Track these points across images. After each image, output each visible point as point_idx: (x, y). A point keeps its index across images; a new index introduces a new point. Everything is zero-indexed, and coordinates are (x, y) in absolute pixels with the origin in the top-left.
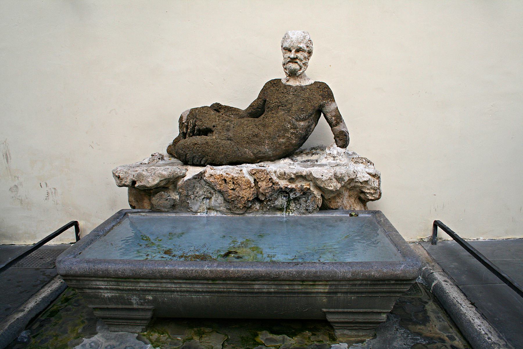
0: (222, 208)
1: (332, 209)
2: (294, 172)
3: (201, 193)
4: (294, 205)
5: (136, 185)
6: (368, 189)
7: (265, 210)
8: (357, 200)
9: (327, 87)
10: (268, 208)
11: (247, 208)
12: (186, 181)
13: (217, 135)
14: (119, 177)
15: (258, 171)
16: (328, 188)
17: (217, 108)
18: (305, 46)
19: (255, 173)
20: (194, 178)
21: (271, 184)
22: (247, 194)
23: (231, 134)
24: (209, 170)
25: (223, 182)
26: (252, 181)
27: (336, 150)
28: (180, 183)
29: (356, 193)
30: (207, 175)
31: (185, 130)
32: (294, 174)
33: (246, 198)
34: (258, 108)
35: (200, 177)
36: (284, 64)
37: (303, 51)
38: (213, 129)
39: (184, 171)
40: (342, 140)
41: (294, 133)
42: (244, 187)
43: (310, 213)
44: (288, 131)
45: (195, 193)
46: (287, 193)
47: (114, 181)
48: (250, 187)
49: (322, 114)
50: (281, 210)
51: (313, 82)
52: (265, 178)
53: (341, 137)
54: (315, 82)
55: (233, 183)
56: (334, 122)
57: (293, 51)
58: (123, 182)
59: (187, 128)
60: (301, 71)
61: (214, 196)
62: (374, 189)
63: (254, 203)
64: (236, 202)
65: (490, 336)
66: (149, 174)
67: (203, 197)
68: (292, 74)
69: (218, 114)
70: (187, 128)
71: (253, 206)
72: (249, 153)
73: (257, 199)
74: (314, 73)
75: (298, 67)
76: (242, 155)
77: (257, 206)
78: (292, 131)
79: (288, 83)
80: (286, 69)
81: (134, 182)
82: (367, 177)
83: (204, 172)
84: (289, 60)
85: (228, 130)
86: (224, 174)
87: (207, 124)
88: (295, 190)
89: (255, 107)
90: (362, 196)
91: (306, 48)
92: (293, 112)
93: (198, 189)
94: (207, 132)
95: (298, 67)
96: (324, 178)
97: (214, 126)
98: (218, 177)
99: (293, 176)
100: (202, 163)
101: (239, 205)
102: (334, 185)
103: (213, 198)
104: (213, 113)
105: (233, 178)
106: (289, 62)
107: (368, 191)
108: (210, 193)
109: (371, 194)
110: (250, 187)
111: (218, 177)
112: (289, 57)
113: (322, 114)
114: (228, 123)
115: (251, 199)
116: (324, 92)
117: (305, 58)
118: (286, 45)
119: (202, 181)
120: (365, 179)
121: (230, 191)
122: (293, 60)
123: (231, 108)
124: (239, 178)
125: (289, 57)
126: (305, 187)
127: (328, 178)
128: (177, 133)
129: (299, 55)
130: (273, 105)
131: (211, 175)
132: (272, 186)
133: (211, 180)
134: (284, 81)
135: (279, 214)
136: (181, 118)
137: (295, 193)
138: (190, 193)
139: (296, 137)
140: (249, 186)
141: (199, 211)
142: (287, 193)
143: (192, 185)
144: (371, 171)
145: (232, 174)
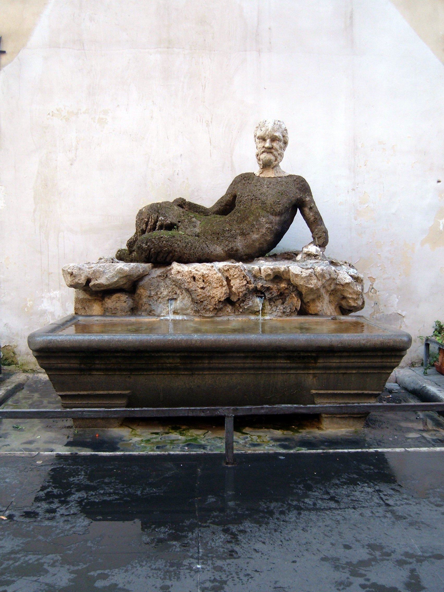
0: (189, 311)
1: (312, 314)
2: (272, 267)
3: (165, 293)
4: (269, 307)
5: (91, 284)
6: (350, 294)
7: (236, 313)
8: (338, 309)
9: (303, 180)
10: (241, 310)
11: (218, 310)
14: (72, 274)
16: (308, 285)
18: (281, 136)
19: (228, 270)
22: (219, 293)
24: (176, 266)
25: (192, 279)
29: (337, 298)
30: (173, 271)
31: (144, 226)
32: (272, 270)
34: (226, 205)
35: (165, 276)
36: (258, 155)
37: (279, 140)
40: (321, 238)
42: (215, 285)
43: (287, 316)
44: (263, 226)
45: (159, 293)
46: (262, 293)
48: (222, 286)
49: (298, 210)
50: (256, 313)
52: (239, 275)
55: (203, 281)
56: (312, 218)
57: (268, 141)
59: (147, 225)
60: (276, 163)
61: (181, 297)
62: (357, 294)
64: (205, 302)
67: (167, 299)
68: (266, 165)
70: (147, 225)
71: (224, 309)
72: (219, 250)
73: (228, 301)
74: (289, 165)
75: (273, 158)
76: (212, 252)
77: (229, 309)
79: (262, 176)
80: (259, 160)
81: (89, 281)
82: (348, 279)
83: (171, 269)
88: (272, 289)
89: (223, 204)
90: (344, 303)
91: (282, 138)
92: (266, 209)
93: (162, 289)
95: (273, 158)
98: (187, 273)
100: (168, 260)
101: (209, 307)
102: (314, 283)
103: (179, 299)
104: (176, 208)
105: (203, 276)
106: (263, 152)
107: (350, 296)
109: (355, 300)
110: (222, 286)
111: (187, 273)
113: (298, 210)
115: (222, 299)
117: (281, 147)
118: (259, 133)
119: (167, 279)
120: (347, 281)
121: (199, 290)
123: (195, 205)
124: (210, 275)
127: (308, 274)
128: (131, 232)
129: (275, 145)
131: (179, 272)
132: (245, 285)
133: (179, 277)
134: (257, 174)
135: (253, 317)
137: (271, 293)
138: (153, 293)
139: (271, 233)
140: (221, 284)
141: (162, 314)
142: (262, 293)
143: (156, 284)
145: (202, 271)
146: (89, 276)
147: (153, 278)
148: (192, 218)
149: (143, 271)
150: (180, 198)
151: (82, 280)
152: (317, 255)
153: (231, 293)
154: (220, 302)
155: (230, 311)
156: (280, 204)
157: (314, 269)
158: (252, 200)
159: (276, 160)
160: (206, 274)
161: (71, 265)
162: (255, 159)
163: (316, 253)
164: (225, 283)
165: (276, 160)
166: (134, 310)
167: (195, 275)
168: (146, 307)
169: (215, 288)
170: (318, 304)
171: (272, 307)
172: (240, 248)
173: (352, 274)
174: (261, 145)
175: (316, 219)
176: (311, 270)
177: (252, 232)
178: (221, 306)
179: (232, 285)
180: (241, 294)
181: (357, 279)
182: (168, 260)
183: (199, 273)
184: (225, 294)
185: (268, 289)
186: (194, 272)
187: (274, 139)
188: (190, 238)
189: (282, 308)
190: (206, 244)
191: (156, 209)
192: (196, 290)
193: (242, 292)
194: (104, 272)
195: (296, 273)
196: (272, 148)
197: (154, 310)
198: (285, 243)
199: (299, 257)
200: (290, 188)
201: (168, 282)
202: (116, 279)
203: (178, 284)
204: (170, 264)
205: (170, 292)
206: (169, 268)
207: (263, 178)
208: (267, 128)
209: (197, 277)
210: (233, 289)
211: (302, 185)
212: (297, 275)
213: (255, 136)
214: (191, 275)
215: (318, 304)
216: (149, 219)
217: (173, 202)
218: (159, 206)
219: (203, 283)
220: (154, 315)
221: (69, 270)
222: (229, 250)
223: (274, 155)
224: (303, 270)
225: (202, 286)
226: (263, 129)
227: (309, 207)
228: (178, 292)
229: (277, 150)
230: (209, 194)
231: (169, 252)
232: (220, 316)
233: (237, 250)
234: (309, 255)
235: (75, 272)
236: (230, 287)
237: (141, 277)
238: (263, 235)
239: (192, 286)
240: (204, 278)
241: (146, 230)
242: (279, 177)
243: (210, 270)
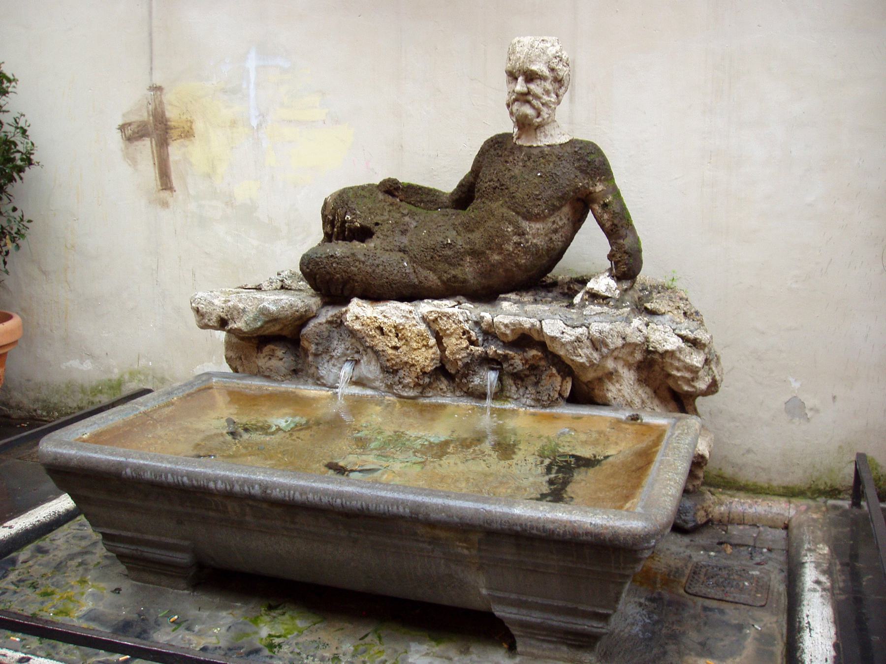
0: (377, 384)
6: (678, 370)
13: (378, 242)
16: (575, 358)
17: (391, 188)
19: (436, 319)
21: (465, 343)
23: (405, 240)
25: (378, 332)
30: (349, 317)
32: (506, 326)
36: (508, 106)
37: (543, 78)
42: (415, 345)
46: (500, 363)
47: (192, 318)
51: (564, 139)
53: (618, 255)
54: (572, 142)
57: (520, 79)
59: (333, 226)
61: (365, 358)
63: (438, 379)
64: (401, 373)
68: (524, 125)
69: (390, 199)
72: (432, 279)
77: (444, 384)
78: (516, 239)
79: (519, 143)
80: (512, 114)
82: (673, 343)
83: (346, 311)
85: (404, 232)
86: (380, 317)
91: (546, 72)
93: (336, 342)
94: (364, 234)
97: (377, 224)
104: (381, 196)
105: (395, 327)
106: (516, 100)
107: (679, 374)
109: (689, 382)
111: (369, 321)
114: (407, 219)
116: (590, 161)
120: (668, 347)
121: (390, 351)
124: (407, 326)
127: (573, 338)
130: (486, 185)
131: (357, 318)
132: (467, 348)
133: (357, 326)
136: (326, 203)
145: (394, 318)
146: (223, 315)
147: (320, 324)
148: (404, 215)
149: (306, 311)
150: (389, 180)
152: (607, 297)
153: (443, 360)
154: (424, 373)
155: (445, 390)
156: (539, 199)
157: (588, 328)
158: (495, 189)
159: (539, 115)
160: (400, 324)
161: (200, 294)
163: (607, 294)
164: (432, 341)
165: (539, 115)
166: (295, 373)
167: (382, 325)
168: (313, 370)
169: (415, 349)
170: (611, 387)
171: (518, 389)
172: (470, 277)
173: (683, 333)
175: (616, 225)
176: (582, 330)
177: (490, 249)
178: (427, 380)
180: (460, 363)
181: (695, 343)
182: (346, 293)
183: (389, 322)
185: (506, 357)
186: (381, 319)
188: (385, 257)
189: (534, 391)
192: (383, 351)
193: (460, 360)
194: (244, 310)
195: (552, 334)
196: (529, 93)
197: (322, 377)
200: (564, 167)
202: (259, 324)
205: (347, 349)
206: (344, 309)
207: (521, 147)
208: (518, 55)
211: (589, 162)
212: (553, 339)
215: (611, 387)
217: (378, 186)
218: (350, 194)
219: (396, 340)
222: (449, 280)
223: (533, 107)
224: (568, 330)
225: (394, 344)
227: (602, 202)
228: (361, 349)
229: (537, 97)
231: (345, 282)
232: (428, 397)
233: (465, 281)
234: (594, 296)
236: (443, 350)
237: (303, 319)
238: (509, 255)
240: (398, 330)
241: (332, 234)
242: (549, 146)
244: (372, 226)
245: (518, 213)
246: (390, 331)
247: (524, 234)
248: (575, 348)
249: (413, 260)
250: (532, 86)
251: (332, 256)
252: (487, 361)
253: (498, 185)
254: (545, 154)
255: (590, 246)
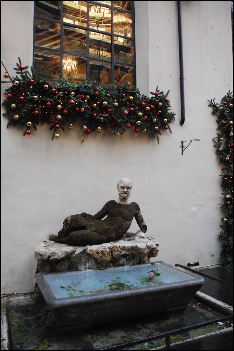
2: (131, 246)
6: (155, 252)
12: (77, 254)
15: (114, 247)
17: (84, 215)
20: (81, 253)
21: (119, 253)
22: (108, 258)
26: (110, 252)
27: (142, 234)
28: (73, 256)
30: (88, 250)
32: (131, 247)
33: (107, 261)
38: (87, 226)
39: (75, 249)
40: (144, 228)
41: (126, 227)
43: (135, 265)
48: (109, 255)
55: (101, 253)
58: (43, 257)
59: (70, 227)
61: (90, 261)
64: (102, 263)
65: (225, 305)
66: (58, 252)
75: (127, 196)
78: (125, 226)
79: (121, 203)
80: (120, 196)
81: (49, 257)
83: (87, 249)
84: (123, 192)
86: (97, 249)
87: (84, 224)
93: (83, 258)
94: (84, 228)
95: (127, 196)
96: (143, 248)
97: (86, 225)
98: (94, 251)
99: (130, 248)
101: (104, 264)
104: (83, 218)
105: (101, 251)
106: (123, 193)
107: (155, 253)
108: (88, 260)
111: (94, 251)
112: (123, 191)
116: (135, 207)
118: (121, 185)
121: (100, 258)
122: (125, 193)
124: (104, 251)
125: (123, 191)
126: (133, 253)
131: (91, 250)
133: (91, 253)
136: (66, 221)
138: (78, 260)
141: (83, 270)
144: (156, 243)
145: (101, 249)
148: (90, 222)
151: (46, 257)
162: (118, 196)
164: (110, 254)
174: (122, 190)
179: (113, 254)
181: (157, 245)
183: (100, 250)
184: (111, 258)
187: (128, 188)
190: (100, 236)
191: (75, 218)
192: (98, 258)
195: (140, 247)
198: (129, 231)
199: (137, 238)
201: (85, 254)
203: (89, 255)
204: (85, 245)
209: (99, 252)
210: (114, 256)
213: (118, 186)
214: (97, 251)
215: (145, 258)
216: (71, 223)
220: (79, 270)
221: (40, 253)
225: (101, 256)
226: (123, 183)
229: (128, 192)
230: (94, 208)
235: (43, 253)
236: (112, 255)
239: (97, 256)
240: (102, 252)
243: (104, 248)
244: (85, 225)
245: (126, 220)
246: (100, 253)
247: (127, 225)
248: (145, 250)
249: (99, 233)
250: (128, 190)
251: (83, 234)
252: (124, 256)
253: (118, 213)
254: (128, 206)
255: (134, 227)
